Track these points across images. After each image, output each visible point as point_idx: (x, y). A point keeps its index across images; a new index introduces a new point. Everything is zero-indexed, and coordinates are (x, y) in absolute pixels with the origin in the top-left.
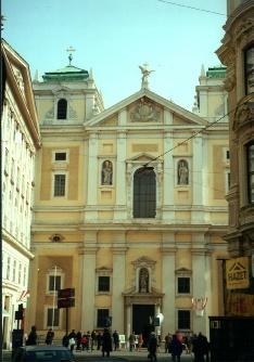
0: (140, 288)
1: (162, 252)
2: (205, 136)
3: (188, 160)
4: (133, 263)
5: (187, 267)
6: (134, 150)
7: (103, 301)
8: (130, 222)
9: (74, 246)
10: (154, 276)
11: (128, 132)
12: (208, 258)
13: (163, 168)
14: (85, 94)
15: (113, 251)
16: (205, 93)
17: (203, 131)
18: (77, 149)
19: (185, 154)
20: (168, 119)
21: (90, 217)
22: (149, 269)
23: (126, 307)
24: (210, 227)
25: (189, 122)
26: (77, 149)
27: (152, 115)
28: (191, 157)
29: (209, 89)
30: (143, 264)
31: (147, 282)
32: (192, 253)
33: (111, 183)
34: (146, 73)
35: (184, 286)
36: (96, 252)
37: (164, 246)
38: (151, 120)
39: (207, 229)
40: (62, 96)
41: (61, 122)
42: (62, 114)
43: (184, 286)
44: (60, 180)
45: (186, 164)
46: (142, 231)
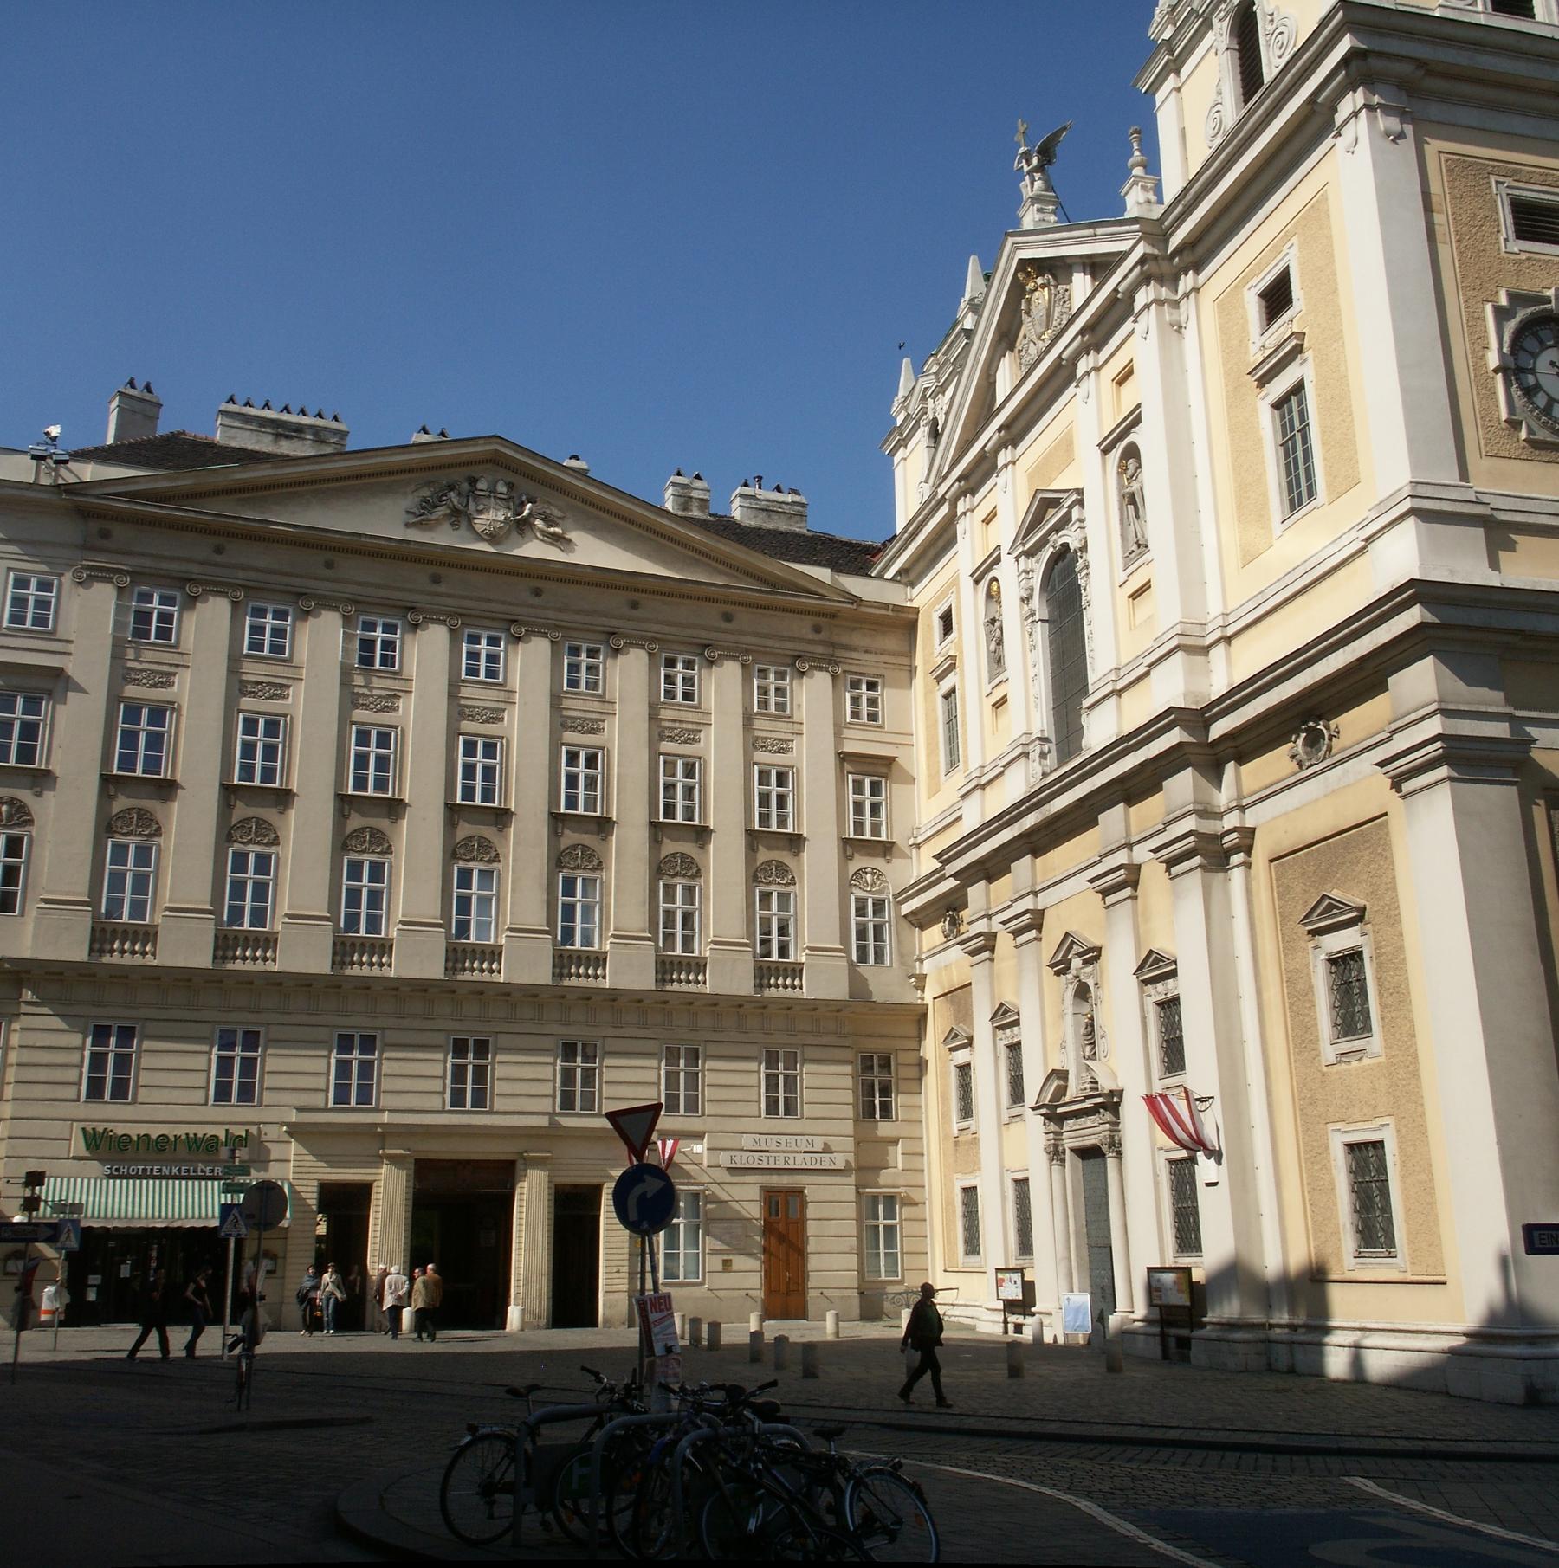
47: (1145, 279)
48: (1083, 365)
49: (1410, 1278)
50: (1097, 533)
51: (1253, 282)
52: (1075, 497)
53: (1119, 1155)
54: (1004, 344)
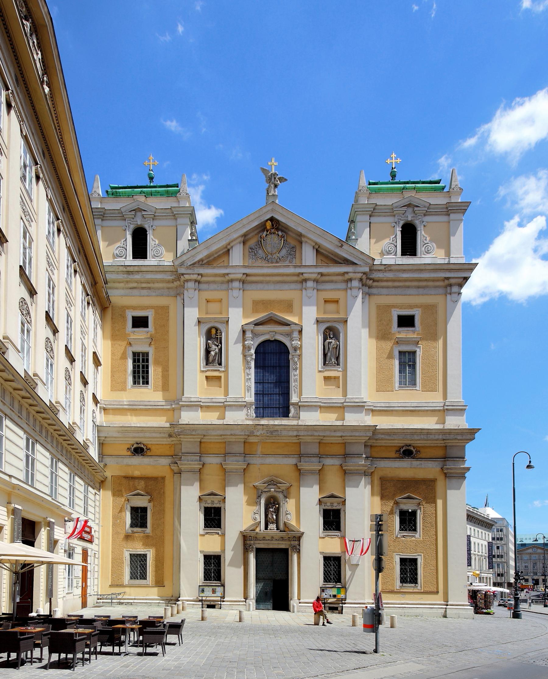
7: (212, 544)
9: (165, 461)
10: (288, 507)
11: (245, 281)
14: (175, 217)
18: (165, 309)
26: (165, 309)
27: (284, 252)
33: (220, 364)
34: (273, 180)
35: (332, 520)
40: (139, 222)
41: (139, 262)
42: (140, 250)
45: (336, 336)
54: (242, 239)
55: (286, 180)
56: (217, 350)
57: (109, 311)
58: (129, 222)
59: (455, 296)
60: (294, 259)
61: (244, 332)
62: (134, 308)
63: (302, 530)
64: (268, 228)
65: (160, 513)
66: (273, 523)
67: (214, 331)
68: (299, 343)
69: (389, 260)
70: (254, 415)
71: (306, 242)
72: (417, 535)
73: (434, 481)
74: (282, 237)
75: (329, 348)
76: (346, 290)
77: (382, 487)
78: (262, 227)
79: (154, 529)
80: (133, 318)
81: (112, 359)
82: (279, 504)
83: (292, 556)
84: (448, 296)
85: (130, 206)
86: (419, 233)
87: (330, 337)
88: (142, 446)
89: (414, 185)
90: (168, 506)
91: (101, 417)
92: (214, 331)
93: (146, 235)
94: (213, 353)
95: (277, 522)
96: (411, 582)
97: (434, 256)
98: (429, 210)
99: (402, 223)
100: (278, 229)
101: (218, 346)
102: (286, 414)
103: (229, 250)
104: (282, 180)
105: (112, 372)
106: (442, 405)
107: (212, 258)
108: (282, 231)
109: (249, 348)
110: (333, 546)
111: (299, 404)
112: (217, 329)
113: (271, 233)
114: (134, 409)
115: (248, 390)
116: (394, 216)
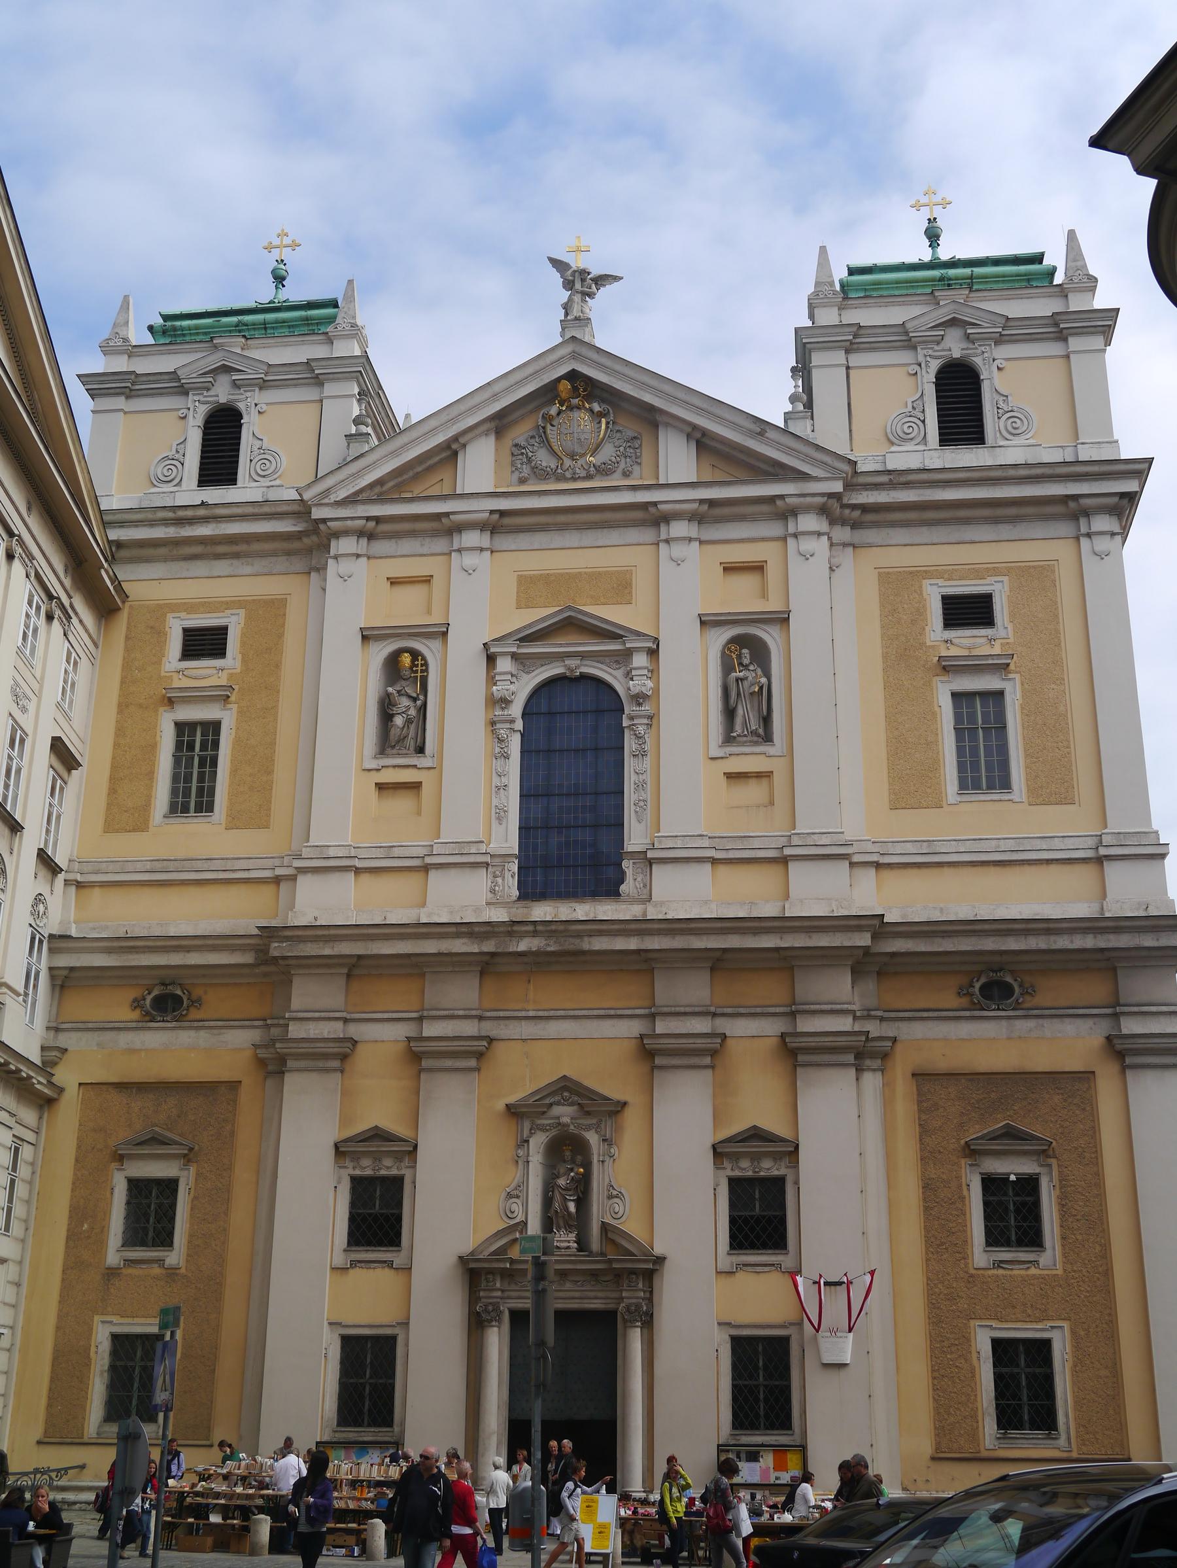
0: (548, 1225)
1: (652, 1056)
2: (842, 534)
3: (770, 636)
4: (514, 1112)
5: (775, 1124)
6: (524, 602)
8: (499, 915)
10: (614, 1169)
11: (499, 524)
12: (872, 1081)
13: (654, 673)
15: (418, 1058)
16: (839, 357)
17: (834, 510)
19: (757, 606)
20: (677, 461)
21: (320, 903)
22: (592, 1138)
23: (477, 1323)
24: (877, 925)
25: (777, 471)
27: (607, 453)
28: (782, 619)
29: (855, 341)
30: (565, 1113)
31: (583, 1201)
32: (796, 1054)
33: (421, 750)
34: (581, 283)
35: (759, 1220)
36: (344, 1057)
37: (661, 1027)
38: (604, 470)
39: (863, 940)
41: (215, 495)
43: (759, 1220)
44: (197, 745)
46: (569, 959)
47: (823, 510)
48: (679, 529)
49: (1075, 1455)
50: (682, 694)
51: (940, 582)
52: (650, 645)
53: (648, 1322)
55: (616, 279)
56: (412, 712)
57: (122, 622)
58: (196, 398)
59: (1102, 544)
60: (636, 468)
61: (491, 659)
62: (190, 607)
63: (658, 1250)
64: (564, 395)
65: (217, 1199)
66: (569, 1227)
67: (406, 659)
68: (650, 684)
69: (904, 459)
70: (515, 893)
71: (667, 425)
72: (1045, 1259)
73: (1087, 1076)
74: (601, 415)
75: (739, 694)
76: (784, 539)
77: (919, 1102)
78: (549, 393)
79: (193, 1251)
80: (185, 630)
81: (116, 745)
82: (587, 1165)
83: (625, 1336)
84: (1084, 542)
85: (202, 363)
86: (986, 388)
87: (740, 664)
88: (179, 992)
89: (967, 271)
90: (242, 1175)
91: (65, 906)
92: (406, 659)
93: (240, 426)
94: (399, 721)
95: (579, 1223)
96: (1035, 1426)
97: (1031, 441)
98: (1009, 332)
99: (935, 365)
100: (589, 398)
101: (415, 700)
102: (610, 889)
103: (455, 454)
104: (602, 280)
105: (113, 779)
106: (1091, 842)
107: (411, 474)
108: (602, 401)
109: (505, 702)
110: (760, 1300)
111: (650, 855)
112: (415, 654)
113: (571, 408)
114: (163, 880)
115: (499, 819)
116: (914, 348)
